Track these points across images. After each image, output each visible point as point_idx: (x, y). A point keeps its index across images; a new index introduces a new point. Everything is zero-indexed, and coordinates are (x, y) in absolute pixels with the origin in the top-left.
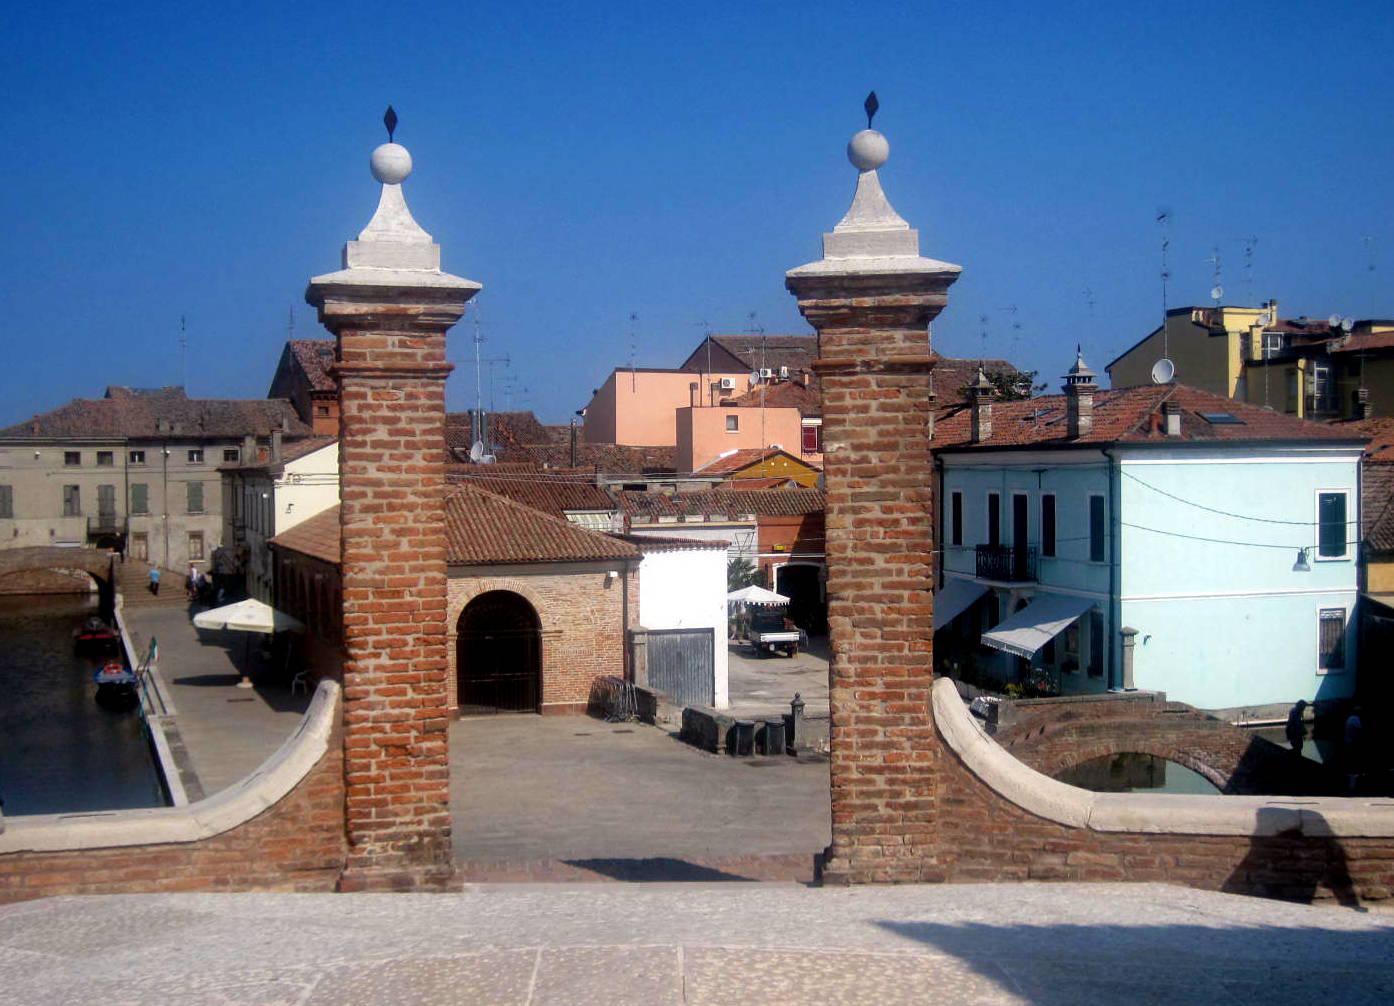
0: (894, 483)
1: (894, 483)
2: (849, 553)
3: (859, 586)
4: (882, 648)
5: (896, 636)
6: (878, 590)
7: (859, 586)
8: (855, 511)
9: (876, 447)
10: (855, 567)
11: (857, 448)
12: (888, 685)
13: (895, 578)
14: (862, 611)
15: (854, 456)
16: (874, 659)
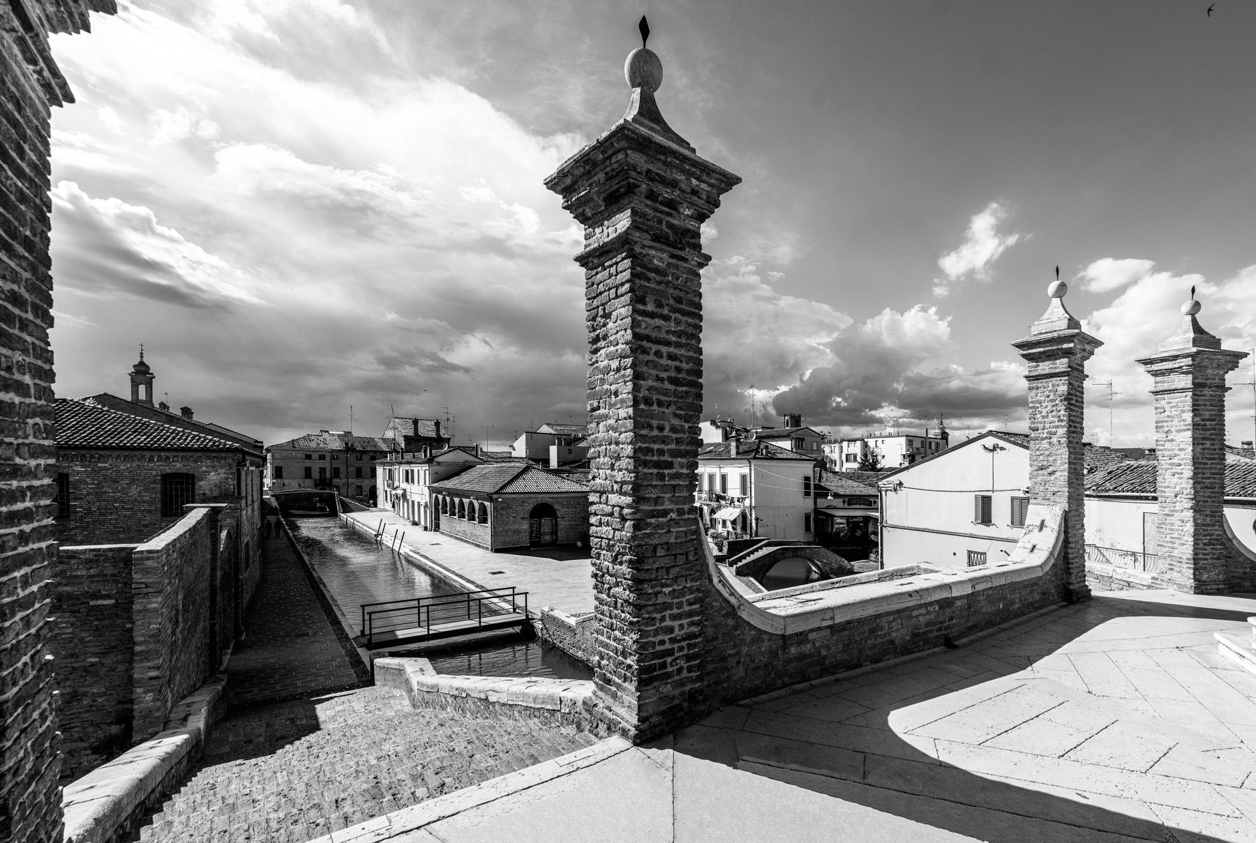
0: (1214, 434)
1: (1214, 434)
2: (1200, 461)
3: (1203, 474)
4: (1210, 497)
5: (1214, 493)
6: (1208, 475)
7: (1203, 474)
8: (1203, 444)
9: (1209, 420)
10: (1202, 466)
11: (1203, 420)
12: (1212, 512)
13: (1214, 471)
14: (1204, 483)
15: (1202, 423)
16: (1207, 501)
